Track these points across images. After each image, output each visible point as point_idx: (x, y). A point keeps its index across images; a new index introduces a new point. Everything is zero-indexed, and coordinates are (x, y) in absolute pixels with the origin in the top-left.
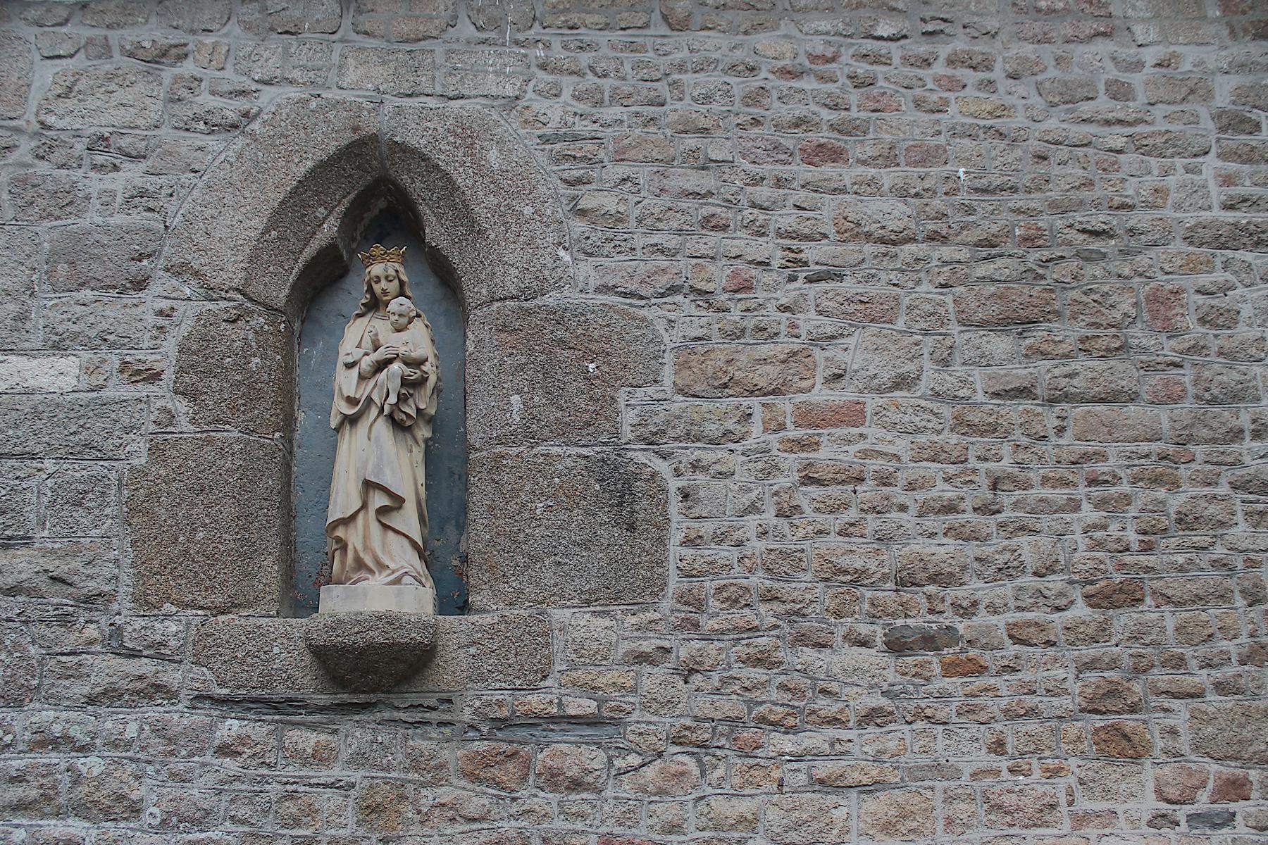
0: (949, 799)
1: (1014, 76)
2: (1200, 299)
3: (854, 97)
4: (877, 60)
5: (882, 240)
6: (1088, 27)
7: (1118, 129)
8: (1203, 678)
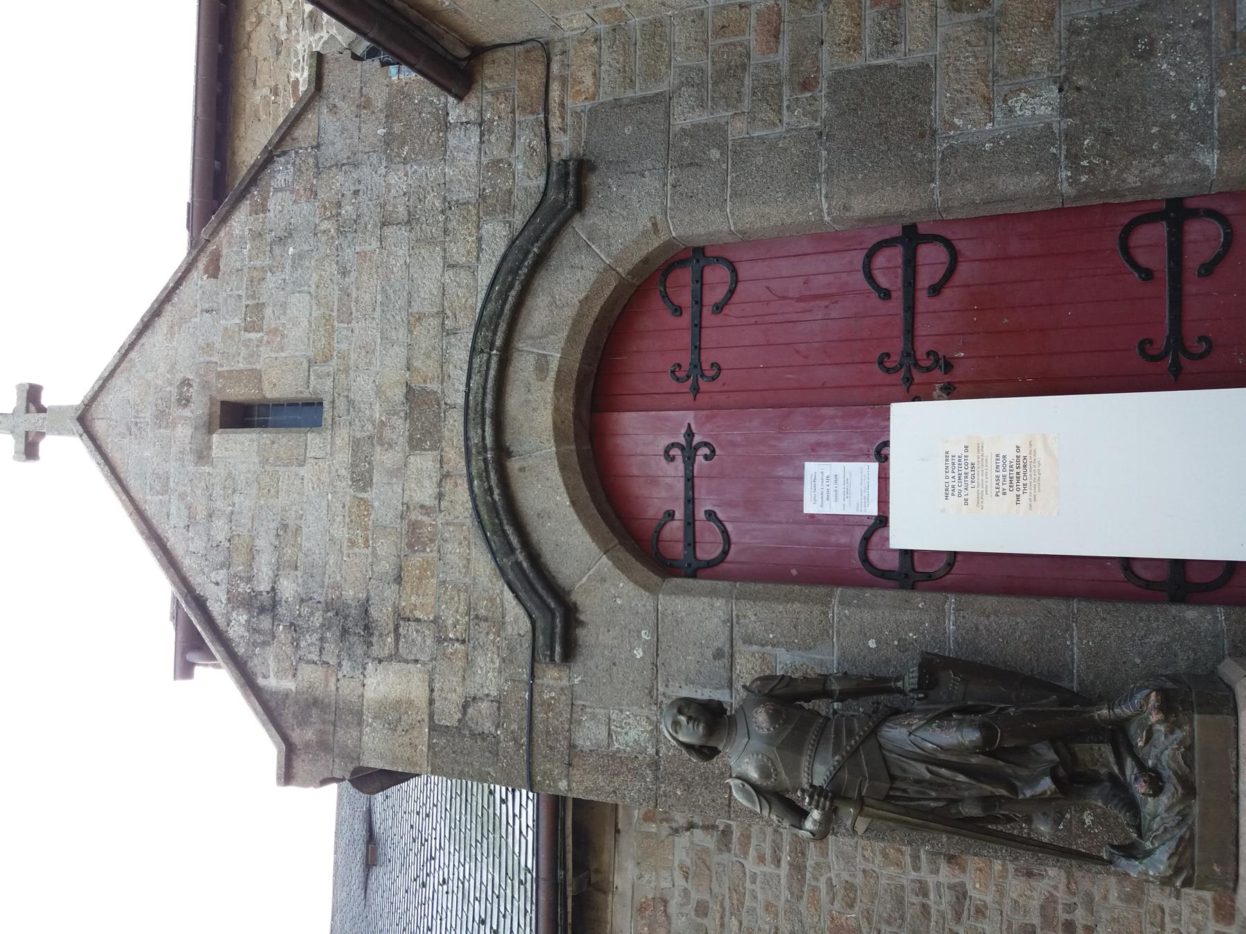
2: (837, 905)
6: (661, 918)
7: (726, 920)
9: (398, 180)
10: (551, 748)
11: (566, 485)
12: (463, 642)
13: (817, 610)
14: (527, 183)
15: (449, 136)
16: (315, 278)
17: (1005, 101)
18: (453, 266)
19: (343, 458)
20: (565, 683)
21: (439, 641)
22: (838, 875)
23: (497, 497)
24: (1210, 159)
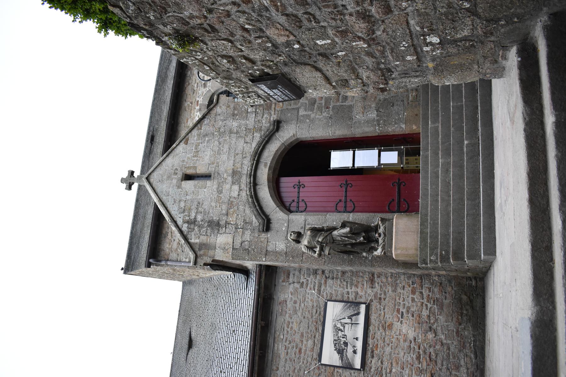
0: (395, 354)
1: (291, 318)
3: (292, 344)
4: (286, 339)
5: (314, 345)
6: (285, 305)
7: (301, 304)
8: (382, 312)
9: (235, 124)
10: (262, 251)
11: (269, 192)
12: (242, 228)
13: (324, 217)
14: (266, 125)
15: (248, 114)
16: (212, 145)
17: (366, 113)
18: (247, 143)
19: (215, 187)
20: (266, 237)
21: (236, 228)
22: (329, 291)
23: (253, 194)
24: (403, 126)
